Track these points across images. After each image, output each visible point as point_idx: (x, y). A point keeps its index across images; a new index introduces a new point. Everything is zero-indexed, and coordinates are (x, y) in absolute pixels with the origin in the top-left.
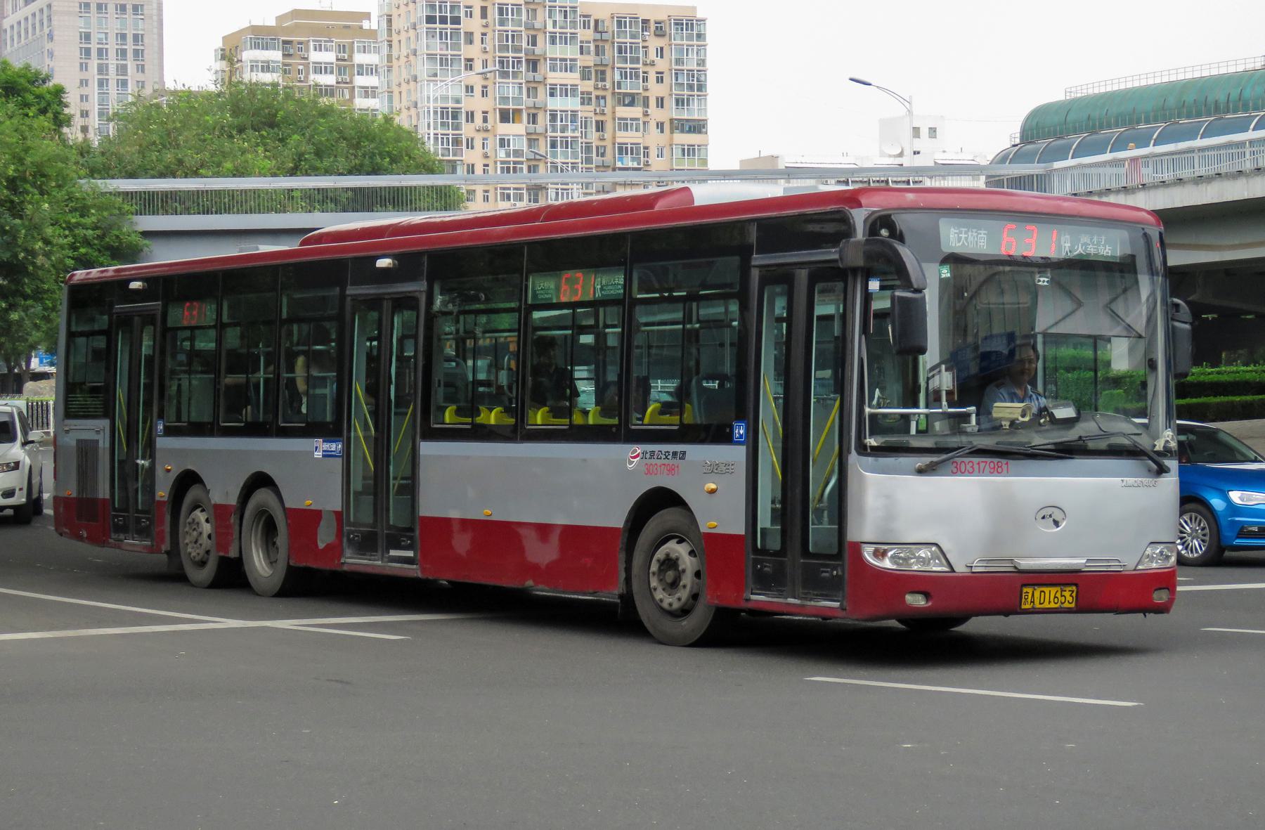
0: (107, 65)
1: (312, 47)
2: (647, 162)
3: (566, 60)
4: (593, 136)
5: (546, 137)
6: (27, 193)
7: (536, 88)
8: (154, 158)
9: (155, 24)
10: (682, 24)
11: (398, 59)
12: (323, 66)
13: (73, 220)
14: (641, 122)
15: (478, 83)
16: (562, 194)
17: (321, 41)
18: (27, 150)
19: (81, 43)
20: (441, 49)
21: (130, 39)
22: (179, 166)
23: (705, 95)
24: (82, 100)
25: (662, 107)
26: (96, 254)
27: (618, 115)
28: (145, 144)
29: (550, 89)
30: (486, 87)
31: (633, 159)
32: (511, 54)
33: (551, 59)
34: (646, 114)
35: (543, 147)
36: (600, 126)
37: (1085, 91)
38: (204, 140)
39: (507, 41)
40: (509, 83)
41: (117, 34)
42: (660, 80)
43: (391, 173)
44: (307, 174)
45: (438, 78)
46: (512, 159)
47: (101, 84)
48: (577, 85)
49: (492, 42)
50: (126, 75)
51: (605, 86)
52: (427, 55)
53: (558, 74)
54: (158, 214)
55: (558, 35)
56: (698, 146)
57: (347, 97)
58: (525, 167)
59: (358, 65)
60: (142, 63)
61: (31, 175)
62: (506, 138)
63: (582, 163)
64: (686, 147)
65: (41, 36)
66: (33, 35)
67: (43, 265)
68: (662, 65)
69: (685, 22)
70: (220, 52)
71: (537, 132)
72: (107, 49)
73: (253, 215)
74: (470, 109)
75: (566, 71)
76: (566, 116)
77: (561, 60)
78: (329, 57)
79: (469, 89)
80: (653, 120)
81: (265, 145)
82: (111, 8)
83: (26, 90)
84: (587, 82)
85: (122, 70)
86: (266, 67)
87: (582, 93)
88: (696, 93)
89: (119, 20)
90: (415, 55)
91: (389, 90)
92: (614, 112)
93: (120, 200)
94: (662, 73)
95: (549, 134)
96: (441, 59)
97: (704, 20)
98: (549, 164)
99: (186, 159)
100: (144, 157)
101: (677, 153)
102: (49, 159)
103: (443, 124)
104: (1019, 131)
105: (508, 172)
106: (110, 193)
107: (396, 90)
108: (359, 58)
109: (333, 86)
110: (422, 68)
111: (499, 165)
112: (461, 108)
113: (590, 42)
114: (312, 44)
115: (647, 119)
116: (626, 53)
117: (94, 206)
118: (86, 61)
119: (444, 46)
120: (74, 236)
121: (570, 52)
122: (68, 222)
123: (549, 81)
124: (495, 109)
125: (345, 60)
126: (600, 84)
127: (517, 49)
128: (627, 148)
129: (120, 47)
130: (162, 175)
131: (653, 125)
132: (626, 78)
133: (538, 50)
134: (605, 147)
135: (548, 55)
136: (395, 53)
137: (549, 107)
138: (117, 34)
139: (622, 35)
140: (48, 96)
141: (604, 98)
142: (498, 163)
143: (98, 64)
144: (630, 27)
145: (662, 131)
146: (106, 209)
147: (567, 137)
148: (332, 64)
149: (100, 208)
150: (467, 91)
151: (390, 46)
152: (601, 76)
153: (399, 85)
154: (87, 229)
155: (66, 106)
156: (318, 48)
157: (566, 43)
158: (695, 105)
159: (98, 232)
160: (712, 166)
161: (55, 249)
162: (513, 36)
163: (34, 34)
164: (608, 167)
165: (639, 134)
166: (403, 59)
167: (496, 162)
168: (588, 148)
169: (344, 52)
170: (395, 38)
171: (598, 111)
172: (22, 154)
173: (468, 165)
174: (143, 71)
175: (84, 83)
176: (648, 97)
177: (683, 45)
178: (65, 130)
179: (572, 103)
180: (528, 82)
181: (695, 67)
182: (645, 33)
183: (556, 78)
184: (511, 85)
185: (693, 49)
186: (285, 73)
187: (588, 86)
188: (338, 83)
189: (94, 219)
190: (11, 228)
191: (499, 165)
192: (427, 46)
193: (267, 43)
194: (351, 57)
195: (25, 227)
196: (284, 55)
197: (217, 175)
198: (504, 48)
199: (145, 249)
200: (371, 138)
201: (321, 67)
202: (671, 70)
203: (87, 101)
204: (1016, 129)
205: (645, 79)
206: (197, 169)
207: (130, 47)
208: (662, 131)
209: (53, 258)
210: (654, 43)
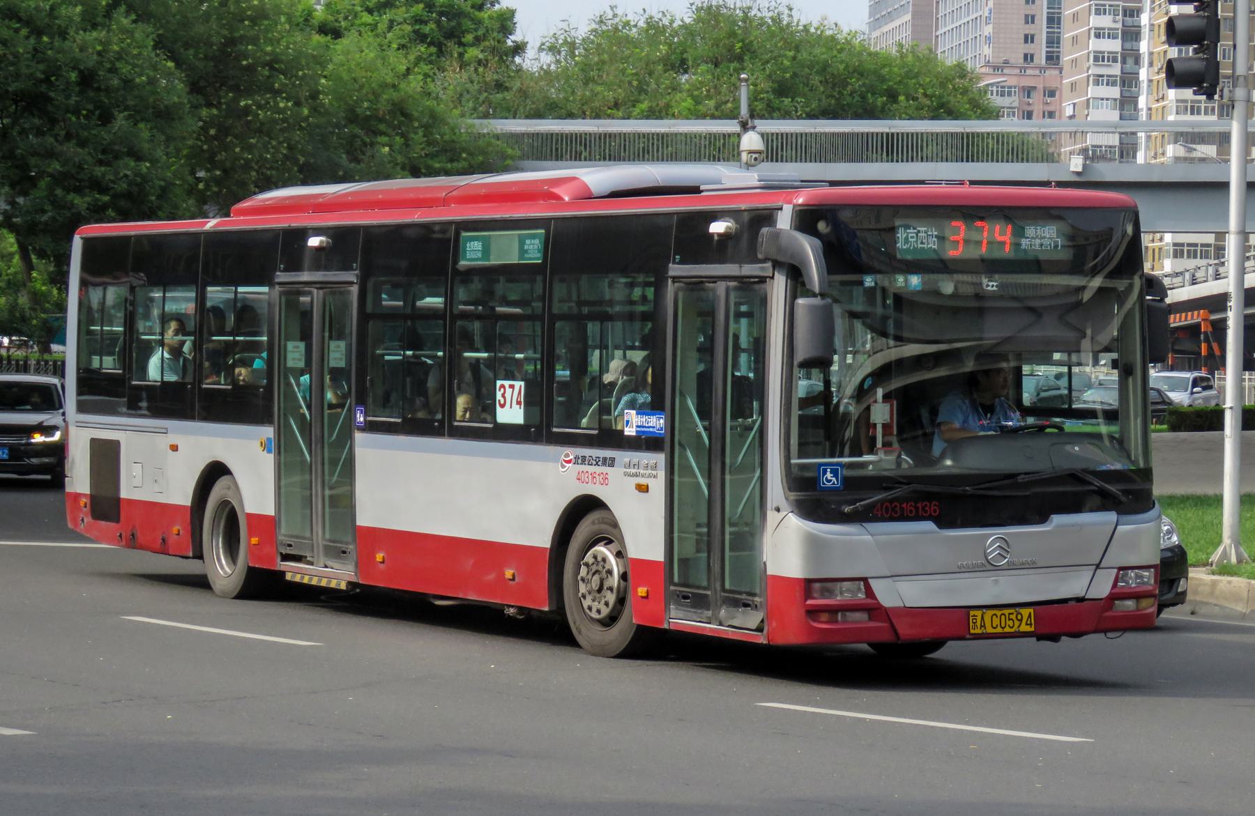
6: (382, 133)
13: (437, 165)
54: (561, 160)
130: (570, 116)
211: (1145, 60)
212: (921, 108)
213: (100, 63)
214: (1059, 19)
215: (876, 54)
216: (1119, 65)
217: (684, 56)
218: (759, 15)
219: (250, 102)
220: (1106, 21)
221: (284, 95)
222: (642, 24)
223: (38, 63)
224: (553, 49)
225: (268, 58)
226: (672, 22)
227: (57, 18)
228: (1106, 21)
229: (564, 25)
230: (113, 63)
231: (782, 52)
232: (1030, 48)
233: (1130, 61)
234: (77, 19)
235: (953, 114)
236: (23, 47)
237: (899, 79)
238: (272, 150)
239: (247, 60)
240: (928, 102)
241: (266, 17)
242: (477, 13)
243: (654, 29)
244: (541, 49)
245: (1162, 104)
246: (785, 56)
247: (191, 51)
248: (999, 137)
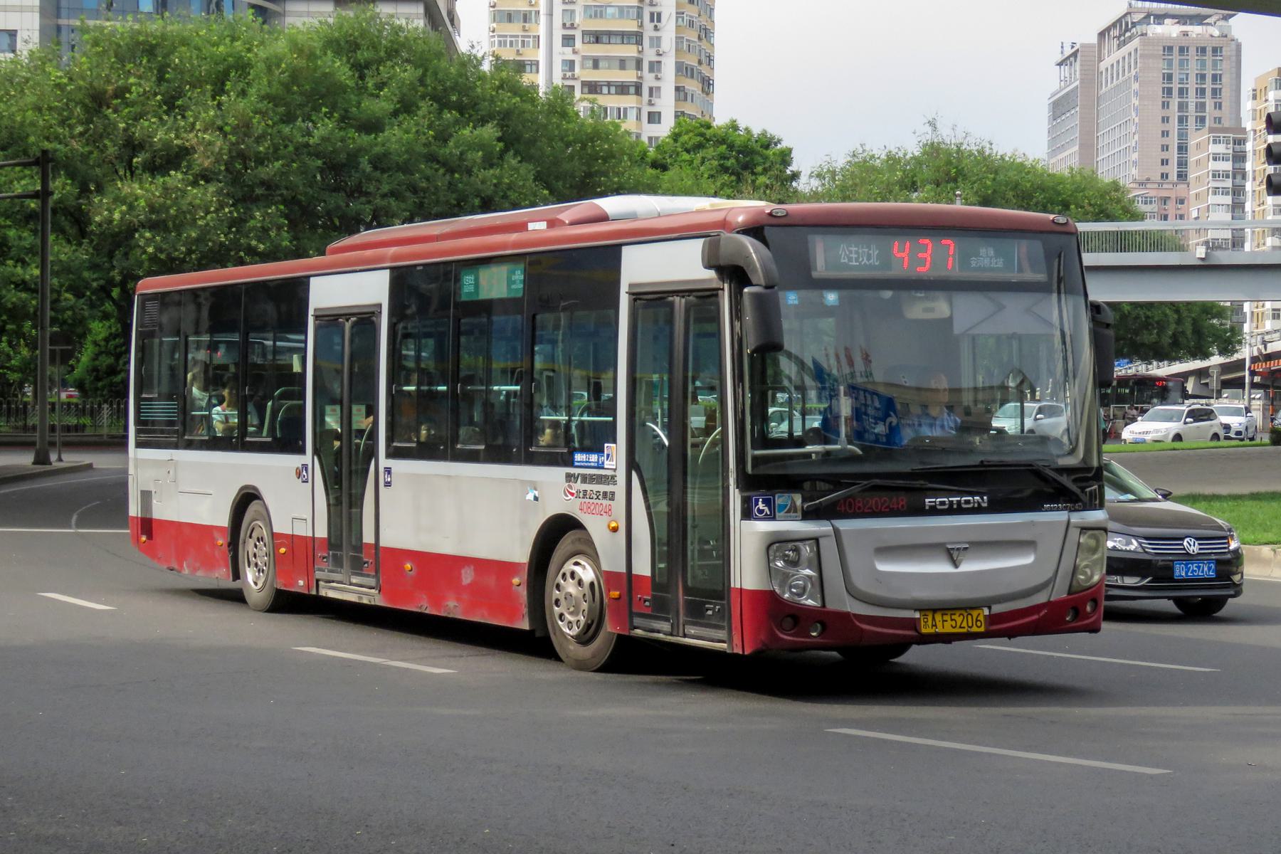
0: (1187, 103)
9: (1234, 64)
21: (1209, 79)
24: (1163, 136)
41: (1197, 74)
47: (1182, 120)
50: (1205, 112)
60: (1220, 100)
65: (1130, 78)
66: (1123, 76)
70: (1251, 93)
72: (1187, 89)
82: (1192, 51)
85: (1201, 107)
89: (1199, 62)
118: (1168, 99)
129: (1199, 86)
138: (1197, 74)
143: (1179, 102)
163: (1123, 75)
174: (1220, 108)
175: (1165, 120)
203: (1167, 136)
207: (1208, 85)
211: (1250, 175)
212: (1086, 213)
213: (496, 192)
214: (1187, 147)
215: (1054, 175)
216: (1230, 180)
217: (915, 179)
218: (968, 148)
220: (1220, 149)
222: (883, 157)
223: (452, 192)
224: (820, 176)
225: (615, 186)
226: (905, 155)
227: (464, 160)
228: (1220, 149)
229: (827, 159)
230: (505, 193)
231: (985, 175)
232: (1165, 169)
233: (1239, 177)
234: (479, 161)
235: (1110, 218)
236: (441, 181)
237: (1070, 193)
239: (600, 187)
240: (1092, 209)
241: (614, 157)
242: (764, 151)
243: (892, 160)
244: (811, 176)
245: (1262, 208)
246: (987, 178)
247: (560, 183)
248: (1144, 234)
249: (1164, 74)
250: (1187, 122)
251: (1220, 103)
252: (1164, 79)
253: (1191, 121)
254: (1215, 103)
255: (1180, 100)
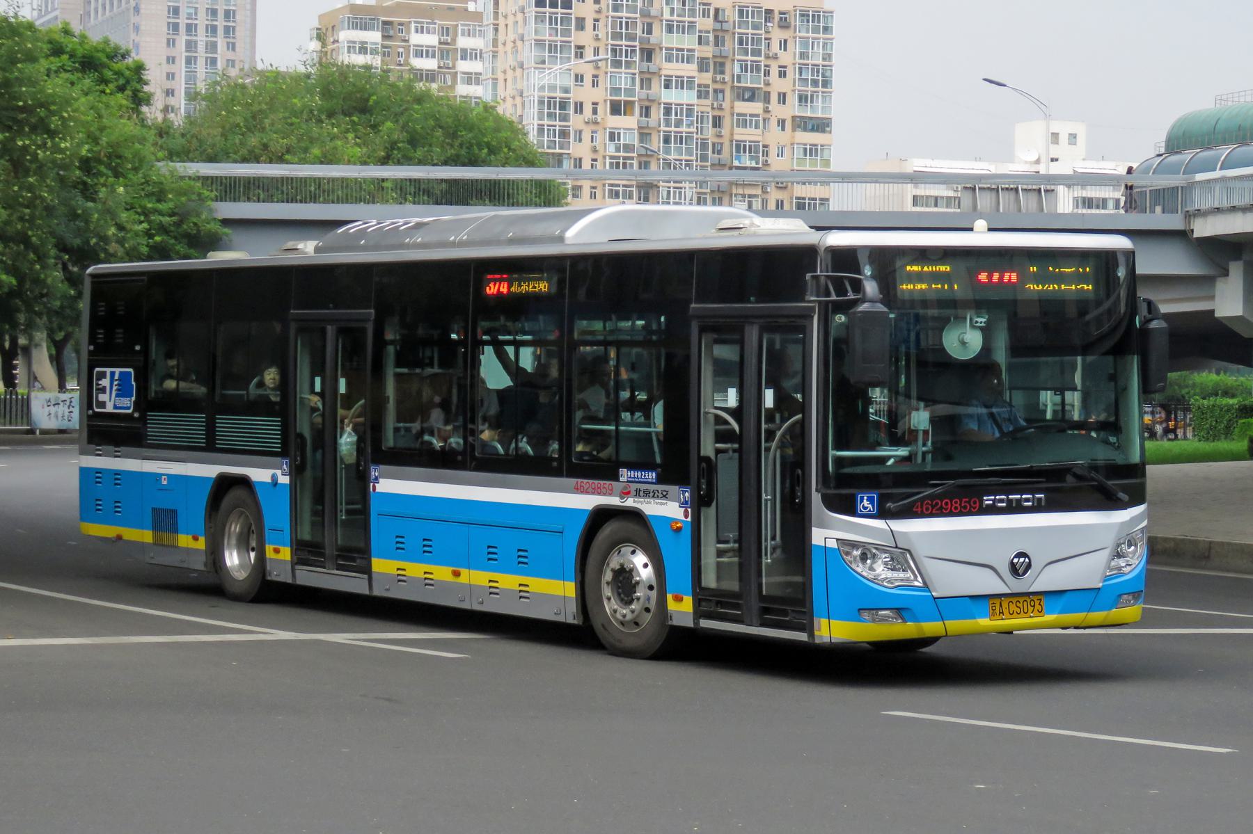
0: (196, 41)
1: (413, 29)
2: (767, 161)
3: (682, 50)
4: (710, 133)
5: (659, 132)
6: (100, 174)
7: (650, 80)
8: (237, 141)
10: (808, 16)
11: (504, 44)
12: (424, 49)
13: (150, 205)
14: (761, 119)
15: (588, 72)
16: (675, 192)
17: (423, 23)
18: (102, 129)
19: (169, 17)
20: (550, 35)
21: (221, 15)
22: (264, 150)
23: (831, 92)
24: (168, 78)
25: (784, 103)
26: (172, 241)
27: (737, 110)
28: (228, 126)
29: (665, 80)
30: (595, 76)
31: (751, 158)
32: (624, 42)
33: (667, 49)
34: (766, 111)
35: (656, 143)
36: (717, 122)
37: (1242, 99)
38: (292, 124)
39: (621, 28)
40: (621, 73)
41: (207, 9)
42: (782, 74)
43: (489, 165)
44: (399, 163)
45: (547, 65)
46: (622, 154)
47: (189, 61)
48: (694, 77)
49: (604, 30)
50: (216, 53)
51: (724, 79)
52: (535, 40)
53: (674, 65)
54: (239, 201)
55: (675, 23)
56: (821, 146)
57: (449, 83)
58: (635, 163)
59: (461, 49)
61: (105, 155)
62: (616, 131)
63: (697, 161)
64: (808, 147)
65: (128, 9)
66: (118, 7)
67: (116, 252)
68: (786, 58)
69: (811, 13)
71: (651, 125)
72: (196, 25)
73: (340, 205)
74: (579, 99)
75: (683, 62)
76: (682, 109)
77: (678, 50)
78: (431, 40)
79: (579, 78)
80: (774, 116)
81: (355, 131)
83: (104, 66)
84: (704, 75)
85: (212, 47)
86: (363, 49)
87: (699, 86)
88: (820, 89)
90: (522, 40)
91: (494, 77)
92: (732, 108)
93: (199, 184)
94: (785, 67)
95: (662, 128)
96: (550, 46)
97: (832, 12)
98: (661, 161)
99: (271, 143)
100: (226, 139)
101: (799, 153)
102: (126, 140)
103: (550, 115)
104: (1164, 139)
105: (618, 167)
106: (190, 178)
107: (500, 76)
108: (463, 42)
109: (434, 71)
110: (529, 54)
111: (608, 161)
112: (569, 99)
113: (709, 32)
114: (413, 25)
115: (767, 116)
116: (747, 44)
117: (171, 191)
118: (174, 37)
119: (554, 32)
120: (150, 222)
121: (688, 41)
122: (144, 208)
123: (664, 72)
124: (605, 101)
125: (448, 44)
126: (719, 77)
127: (631, 37)
128: (745, 146)
130: (244, 160)
131: (773, 122)
132: (746, 71)
133: (653, 39)
134: (722, 144)
135: (664, 45)
136: (501, 38)
137: (663, 100)
139: (743, 25)
140: (127, 73)
141: (722, 91)
142: (607, 158)
144: (753, 17)
145: (783, 129)
146: (185, 194)
147: (682, 133)
148: (435, 47)
149: (180, 193)
150: (576, 81)
151: (496, 30)
152: (720, 67)
153: (505, 72)
154: (163, 215)
155: (146, 84)
156: (420, 30)
157: (683, 33)
158: (819, 103)
159: (175, 219)
160: (835, 167)
161: (129, 235)
162: (627, 23)
164: (725, 165)
165: (759, 131)
166: (509, 45)
167: (604, 157)
168: (704, 146)
169: (447, 35)
170: (501, 21)
171: (715, 106)
172: (97, 133)
173: (575, 159)
174: (234, 49)
175: (171, 60)
176: (769, 92)
177: (808, 38)
178: (144, 109)
179: (687, 97)
180: (641, 72)
181: (820, 62)
182: (768, 24)
183: (672, 69)
184: (623, 76)
185: (818, 43)
186: (384, 55)
187: (707, 78)
188: (439, 67)
189: (171, 205)
190: (83, 211)
191: (608, 161)
192: (535, 31)
193: (366, 23)
194: (454, 40)
195: (98, 211)
196: (385, 37)
197: (303, 161)
198: (617, 36)
199: (224, 237)
200: (471, 128)
201: (422, 51)
202: (794, 64)
203: (173, 78)
204: (1162, 138)
205: (767, 73)
206: (283, 154)
207: (220, 23)
208: (783, 129)
209: (127, 245)
210: (777, 35)
219: (27, 142)
221: (61, 136)
238: (46, 189)
249: (169, 6)
250: (195, 64)
251: (234, 44)
252: (169, 13)
253: (201, 63)
254: (228, 43)
255: (189, 38)
